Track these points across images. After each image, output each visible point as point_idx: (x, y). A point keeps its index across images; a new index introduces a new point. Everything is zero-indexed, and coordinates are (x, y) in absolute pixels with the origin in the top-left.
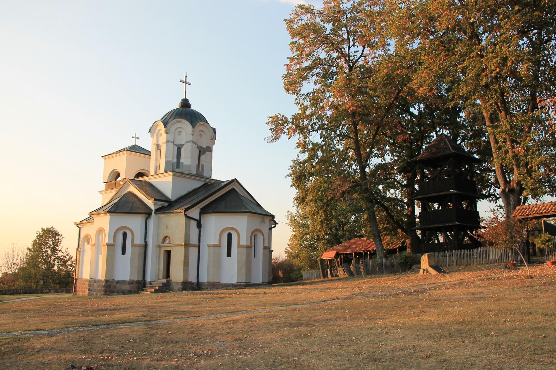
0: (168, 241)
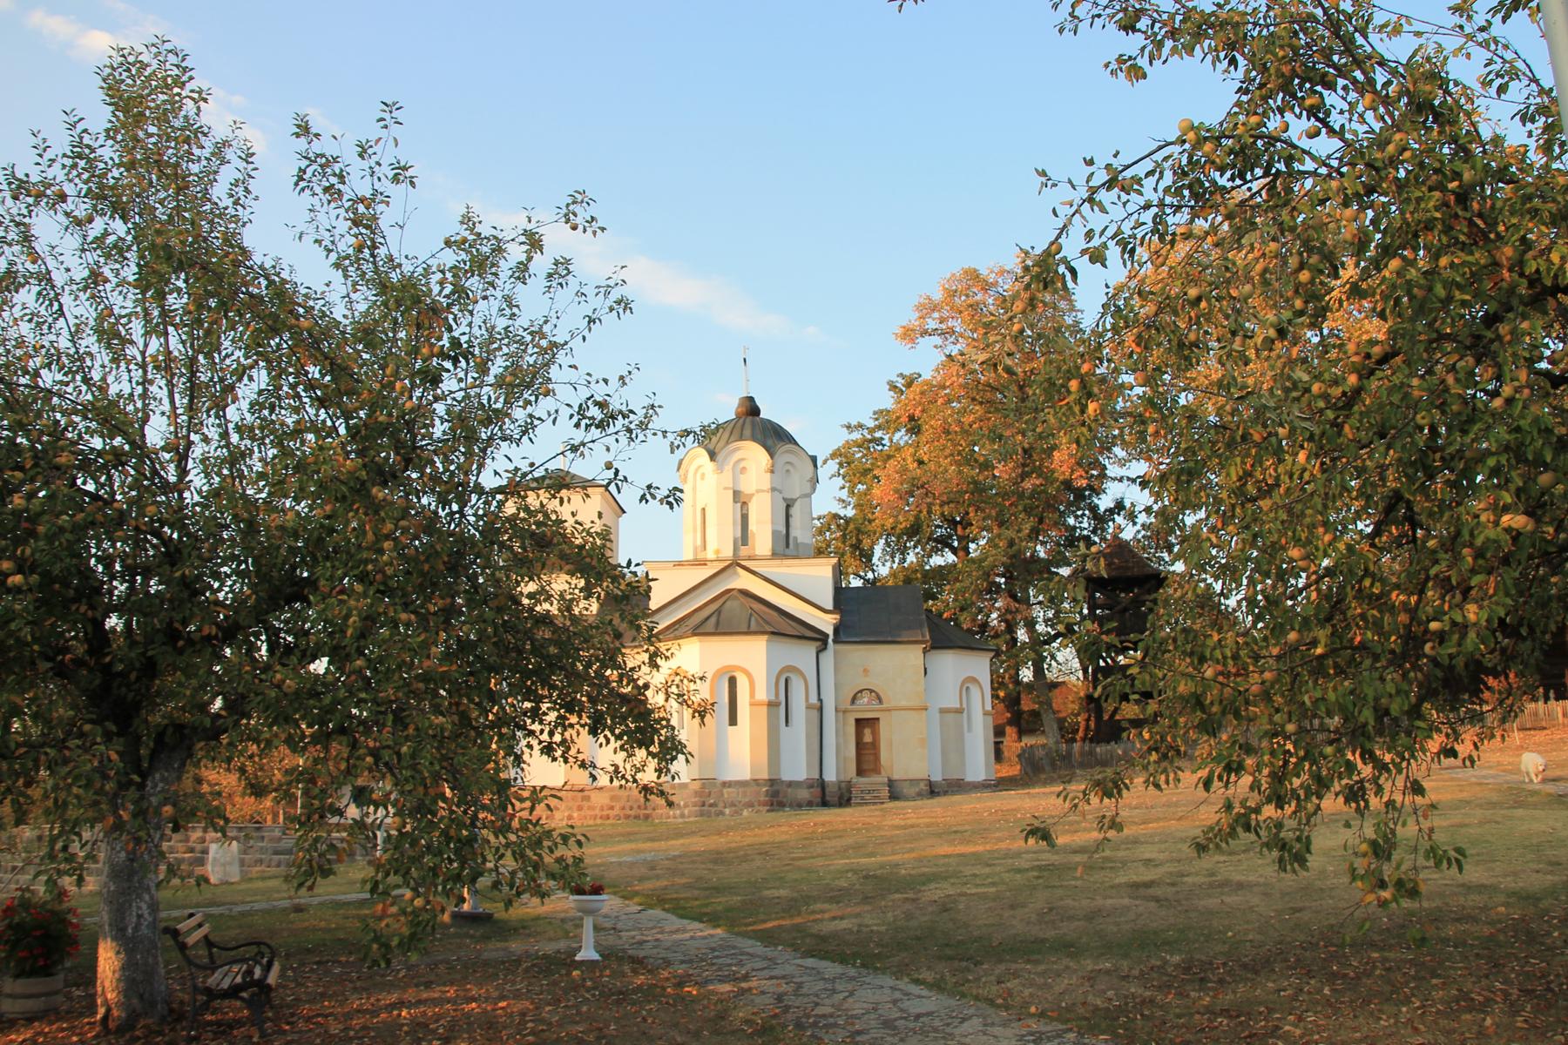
0: (866, 700)
